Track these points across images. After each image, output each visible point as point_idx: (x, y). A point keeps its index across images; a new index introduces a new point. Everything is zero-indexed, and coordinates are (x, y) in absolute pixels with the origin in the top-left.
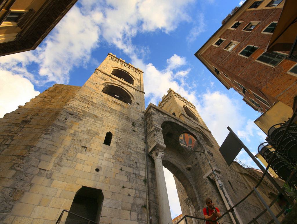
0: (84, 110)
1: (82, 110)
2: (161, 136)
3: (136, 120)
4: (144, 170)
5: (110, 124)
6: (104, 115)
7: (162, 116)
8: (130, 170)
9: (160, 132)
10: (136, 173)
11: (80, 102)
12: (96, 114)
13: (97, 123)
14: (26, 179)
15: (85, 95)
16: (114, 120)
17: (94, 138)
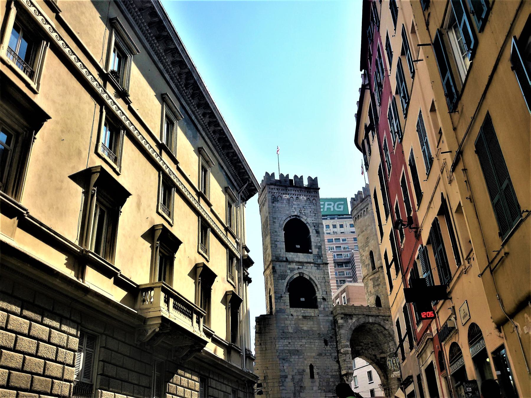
0: (288, 348)
1: (287, 350)
5: (309, 354)
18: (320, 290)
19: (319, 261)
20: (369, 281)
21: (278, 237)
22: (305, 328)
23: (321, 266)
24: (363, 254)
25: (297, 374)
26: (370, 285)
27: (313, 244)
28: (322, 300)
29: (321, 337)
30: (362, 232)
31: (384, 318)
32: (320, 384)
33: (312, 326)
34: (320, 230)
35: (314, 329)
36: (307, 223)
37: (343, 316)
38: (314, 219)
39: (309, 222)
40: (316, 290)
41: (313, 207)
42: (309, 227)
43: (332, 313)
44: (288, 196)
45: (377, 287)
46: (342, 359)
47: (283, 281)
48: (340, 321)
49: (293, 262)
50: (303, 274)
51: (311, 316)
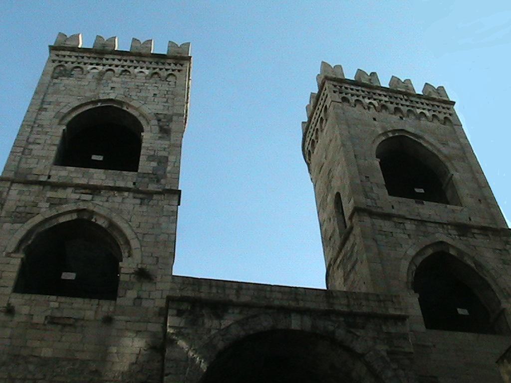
7: (216, 323)
18: (137, 254)
19: (152, 187)
21: (44, 137)
22: (47, 352)
23: (155, 197)
30: (320, 173)
34: (173, 126)
35: (78, 356)
36: (141, 114)
37: (185, 306)
38: (162, 107)
42: (143, 122)
44: (100, 68)
47: (17, 226)
49: (64, 186)
50: (92, 213)
51: (77, 320)
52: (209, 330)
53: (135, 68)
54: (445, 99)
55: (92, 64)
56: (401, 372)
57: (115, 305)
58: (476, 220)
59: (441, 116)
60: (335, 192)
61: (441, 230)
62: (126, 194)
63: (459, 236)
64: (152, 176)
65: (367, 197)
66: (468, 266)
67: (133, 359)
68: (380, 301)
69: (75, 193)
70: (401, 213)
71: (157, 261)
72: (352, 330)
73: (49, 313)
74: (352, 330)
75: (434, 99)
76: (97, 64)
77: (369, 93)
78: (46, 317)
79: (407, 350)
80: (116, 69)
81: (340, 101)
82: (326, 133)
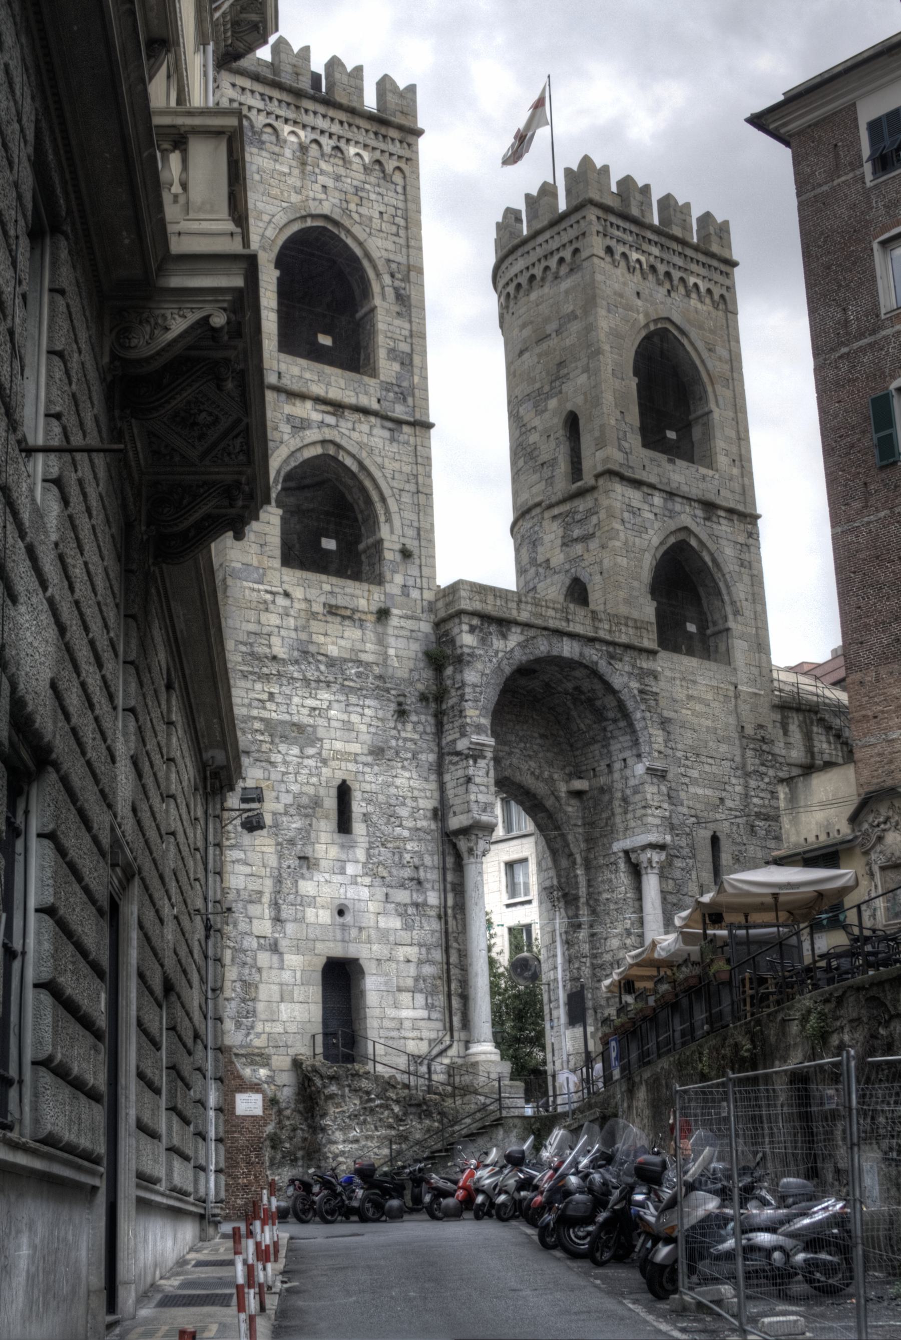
0: (265, 714)
1: (262, 720)
2: (487, 773)
3: (406, 676)
4: (436, 886)
5: (338, 745)
6: (314, 709)
7: (502, 642)
8: (403, 896)
9: (485, 758)
10: (420, 900)
11: (249, 685)
12: (295, 719)
13: (308, 757)
14: (249, 960)
15: (250, 633)
16: (345, 717)
17: (314, 820)
19: (399, 411)
20: (546, 523)
22: (333, 651)
23: (406, 429)
24: (537, 422)
25: (292, 811)
26: (547, 538)
27: (383, 344)
28: (398, 557)
29: (387, 691)
31: (611, 649)
32: (369, 856)
33: (358, 645)
35: (364, 657)
37: (476, 621)
38: (391, 247)
39: (375, 254)
40: (382, 518)
41: (393, 199)
43: (431, 608)
44: (302, 133)
45: (579, 548)
46: (460, 773)
48: (467, 640)
49: (303, 397)
50: (339, 446)
51: (355, 611)
52: (497, 652)
53: (348, 141)
54: (727, 256)
55: (286, 121)
56: (648, 714)
57: (385, 594)
58: (727, 499)
59: (717, 292)
60: (569, 406)
61: (688, 509)
62: (373, 419)
63: (705, 519)
64: (396, 389)
65: (620, 448)
66: (705, 563)
67: (412, 666)
68: (636, 628)
69: (316, 410)
70: (653, 479)
71: (419, 534)
72: (613, 662)
73: (323, 599)
74: (613, 662)
75: (713, 256)
76: (295, 123)
77: (637, 235)
78: (324, 604)
79: (654, 689)
80: (324, 140)
81: (602, 253)
82: (567, 292)
